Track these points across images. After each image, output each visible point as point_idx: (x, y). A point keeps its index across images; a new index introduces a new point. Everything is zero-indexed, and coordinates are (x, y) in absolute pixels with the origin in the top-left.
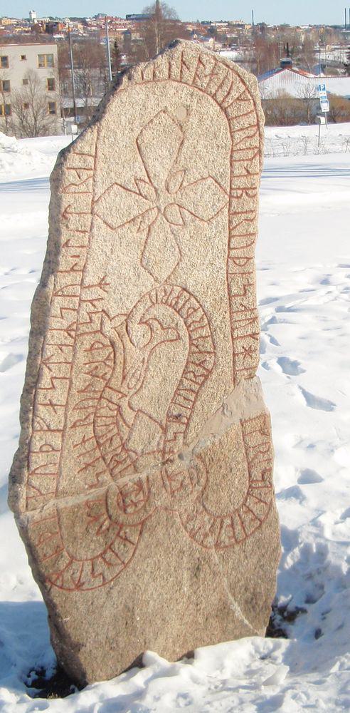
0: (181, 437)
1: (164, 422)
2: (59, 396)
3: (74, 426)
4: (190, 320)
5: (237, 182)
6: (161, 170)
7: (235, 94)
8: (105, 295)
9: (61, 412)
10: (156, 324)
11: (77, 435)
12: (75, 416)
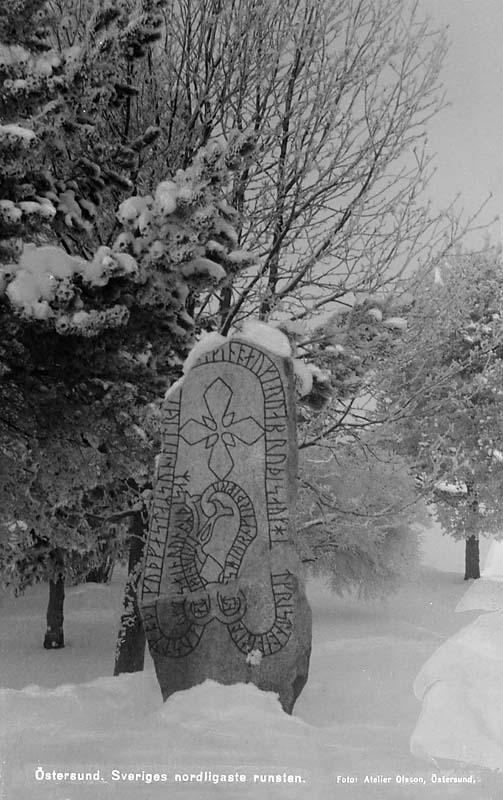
0: (233, 576)
1: (223, 565)
2: (161, 537)
3: (169, 556)
4: (240, 504)
5: (268, 422)
6: (218, 412)
7: (265, 368)
8: (186, 482)
9: (162, 546)
10: (218, 504)
11: (169, 562)
12: (168, 551)
